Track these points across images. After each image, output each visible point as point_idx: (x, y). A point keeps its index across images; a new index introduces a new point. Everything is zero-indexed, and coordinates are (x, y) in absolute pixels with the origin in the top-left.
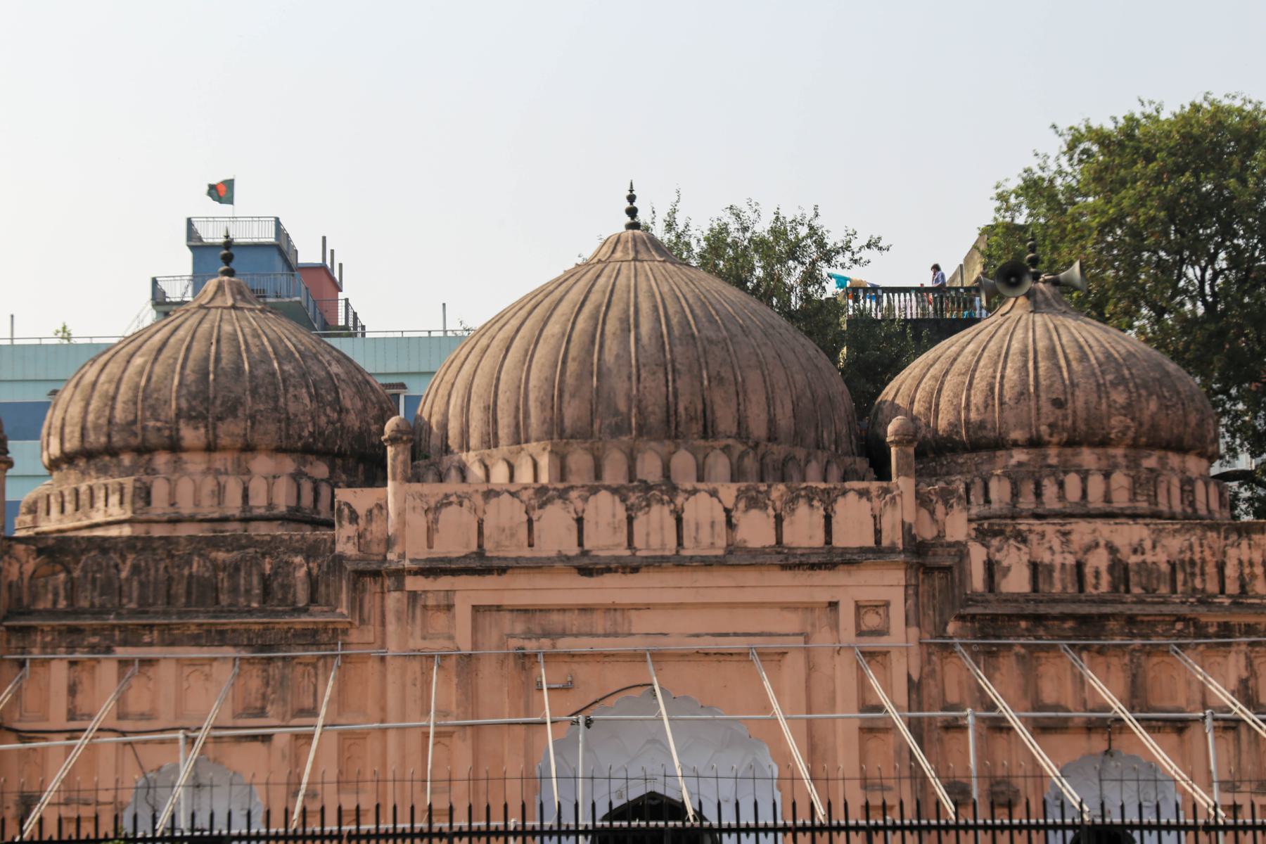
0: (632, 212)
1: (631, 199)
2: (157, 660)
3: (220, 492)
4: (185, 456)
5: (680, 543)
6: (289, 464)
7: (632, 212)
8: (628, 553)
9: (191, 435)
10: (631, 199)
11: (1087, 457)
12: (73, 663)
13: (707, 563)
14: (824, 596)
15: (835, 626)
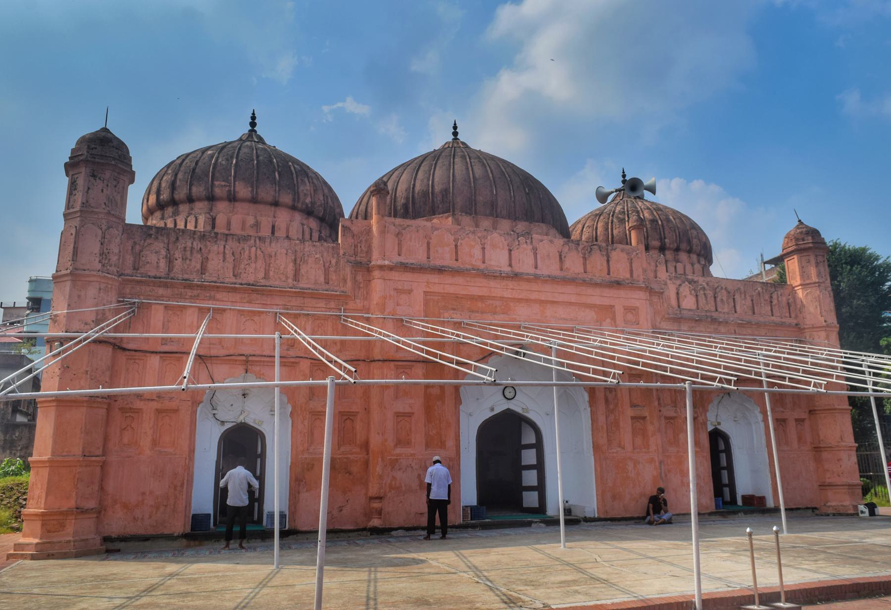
0: (455, 134)
1: (455, 127)
2: (224, 310)
3: (257, 225)
4: (237, 204)
5: (536, 268)
6: (298, 217)
7: (455, 134)
8: (510, 269)
9: (243, 190)
10: (455, 127)
11: (683, 256)
12: (167, 307)
13: (552, 280)
14: (607, 302)
15: (614, 319)
